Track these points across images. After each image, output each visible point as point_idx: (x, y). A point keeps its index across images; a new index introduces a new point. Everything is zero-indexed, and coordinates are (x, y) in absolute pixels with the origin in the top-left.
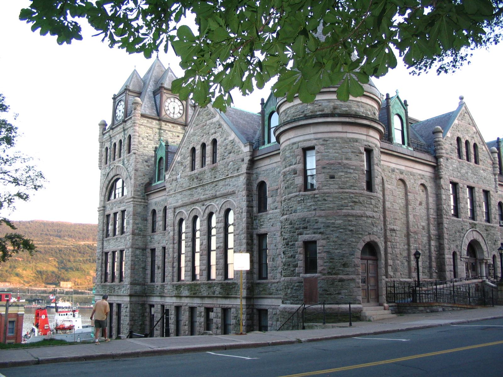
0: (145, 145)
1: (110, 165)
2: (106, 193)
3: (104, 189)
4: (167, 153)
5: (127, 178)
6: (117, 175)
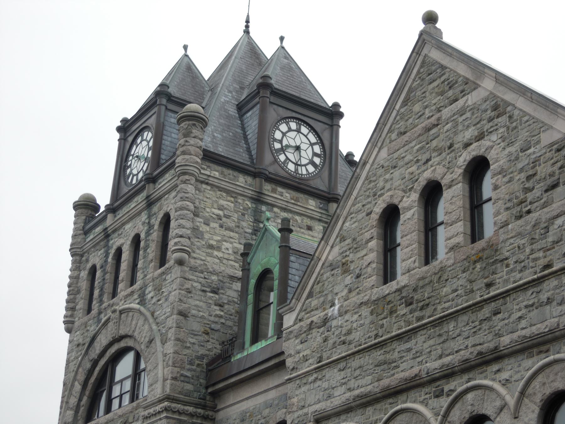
0: (214, 243)
1: (100, 313)
2: (80, 400)
3: (78, 387)
4: (286, 250)
5: (151, 341)
6: (122, 338)
